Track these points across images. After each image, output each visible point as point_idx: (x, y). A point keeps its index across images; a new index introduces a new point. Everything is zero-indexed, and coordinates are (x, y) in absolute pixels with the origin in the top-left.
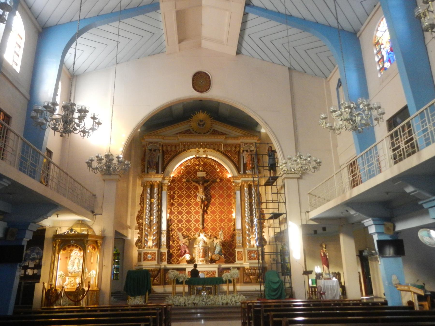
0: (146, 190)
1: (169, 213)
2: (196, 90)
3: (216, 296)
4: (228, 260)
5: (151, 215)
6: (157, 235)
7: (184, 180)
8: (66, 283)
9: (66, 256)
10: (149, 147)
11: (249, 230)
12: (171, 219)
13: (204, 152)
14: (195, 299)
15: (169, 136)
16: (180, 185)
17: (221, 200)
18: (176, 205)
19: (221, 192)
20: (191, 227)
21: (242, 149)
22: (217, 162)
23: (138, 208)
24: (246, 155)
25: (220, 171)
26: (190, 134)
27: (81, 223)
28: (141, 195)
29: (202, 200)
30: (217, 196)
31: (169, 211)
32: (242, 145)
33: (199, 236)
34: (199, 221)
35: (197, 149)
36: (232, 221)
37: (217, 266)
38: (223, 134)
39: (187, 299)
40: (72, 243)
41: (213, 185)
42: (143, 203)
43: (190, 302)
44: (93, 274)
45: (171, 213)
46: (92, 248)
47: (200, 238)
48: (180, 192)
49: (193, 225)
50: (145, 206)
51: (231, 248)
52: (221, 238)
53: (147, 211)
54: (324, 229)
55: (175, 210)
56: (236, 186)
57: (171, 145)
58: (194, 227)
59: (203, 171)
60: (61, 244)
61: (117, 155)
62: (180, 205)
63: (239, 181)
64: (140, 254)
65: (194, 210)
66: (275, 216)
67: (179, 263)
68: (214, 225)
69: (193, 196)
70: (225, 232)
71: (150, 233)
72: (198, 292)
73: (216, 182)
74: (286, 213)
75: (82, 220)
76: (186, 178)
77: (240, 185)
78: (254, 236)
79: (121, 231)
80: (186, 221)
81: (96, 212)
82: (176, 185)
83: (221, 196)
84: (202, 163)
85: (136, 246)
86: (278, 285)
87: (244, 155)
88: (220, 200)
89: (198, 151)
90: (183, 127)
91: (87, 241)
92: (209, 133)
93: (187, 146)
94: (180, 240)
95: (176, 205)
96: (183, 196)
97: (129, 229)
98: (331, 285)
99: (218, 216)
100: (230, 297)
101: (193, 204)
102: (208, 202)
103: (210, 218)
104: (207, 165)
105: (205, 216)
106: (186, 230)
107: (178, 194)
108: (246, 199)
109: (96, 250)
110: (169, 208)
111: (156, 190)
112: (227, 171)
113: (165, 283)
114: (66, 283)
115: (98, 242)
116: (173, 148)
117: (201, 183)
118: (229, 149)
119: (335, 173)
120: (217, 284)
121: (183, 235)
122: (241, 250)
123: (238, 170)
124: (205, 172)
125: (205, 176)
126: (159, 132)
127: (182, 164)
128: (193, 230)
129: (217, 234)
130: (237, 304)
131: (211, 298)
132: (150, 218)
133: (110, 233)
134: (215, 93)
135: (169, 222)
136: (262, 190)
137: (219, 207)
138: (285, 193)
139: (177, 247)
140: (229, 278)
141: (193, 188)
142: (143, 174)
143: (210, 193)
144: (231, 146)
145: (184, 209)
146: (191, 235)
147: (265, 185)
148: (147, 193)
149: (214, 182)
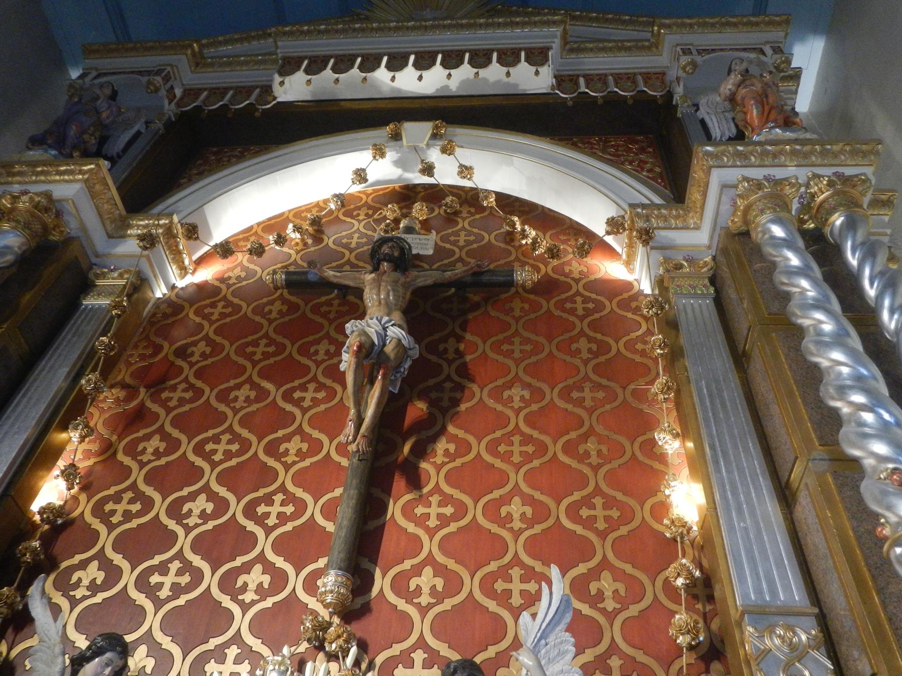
68: (471, 585)
87: (702, 113)
99: (516, 508)
102: (432, 403)
105: (395, 510)
137: (527, 440)
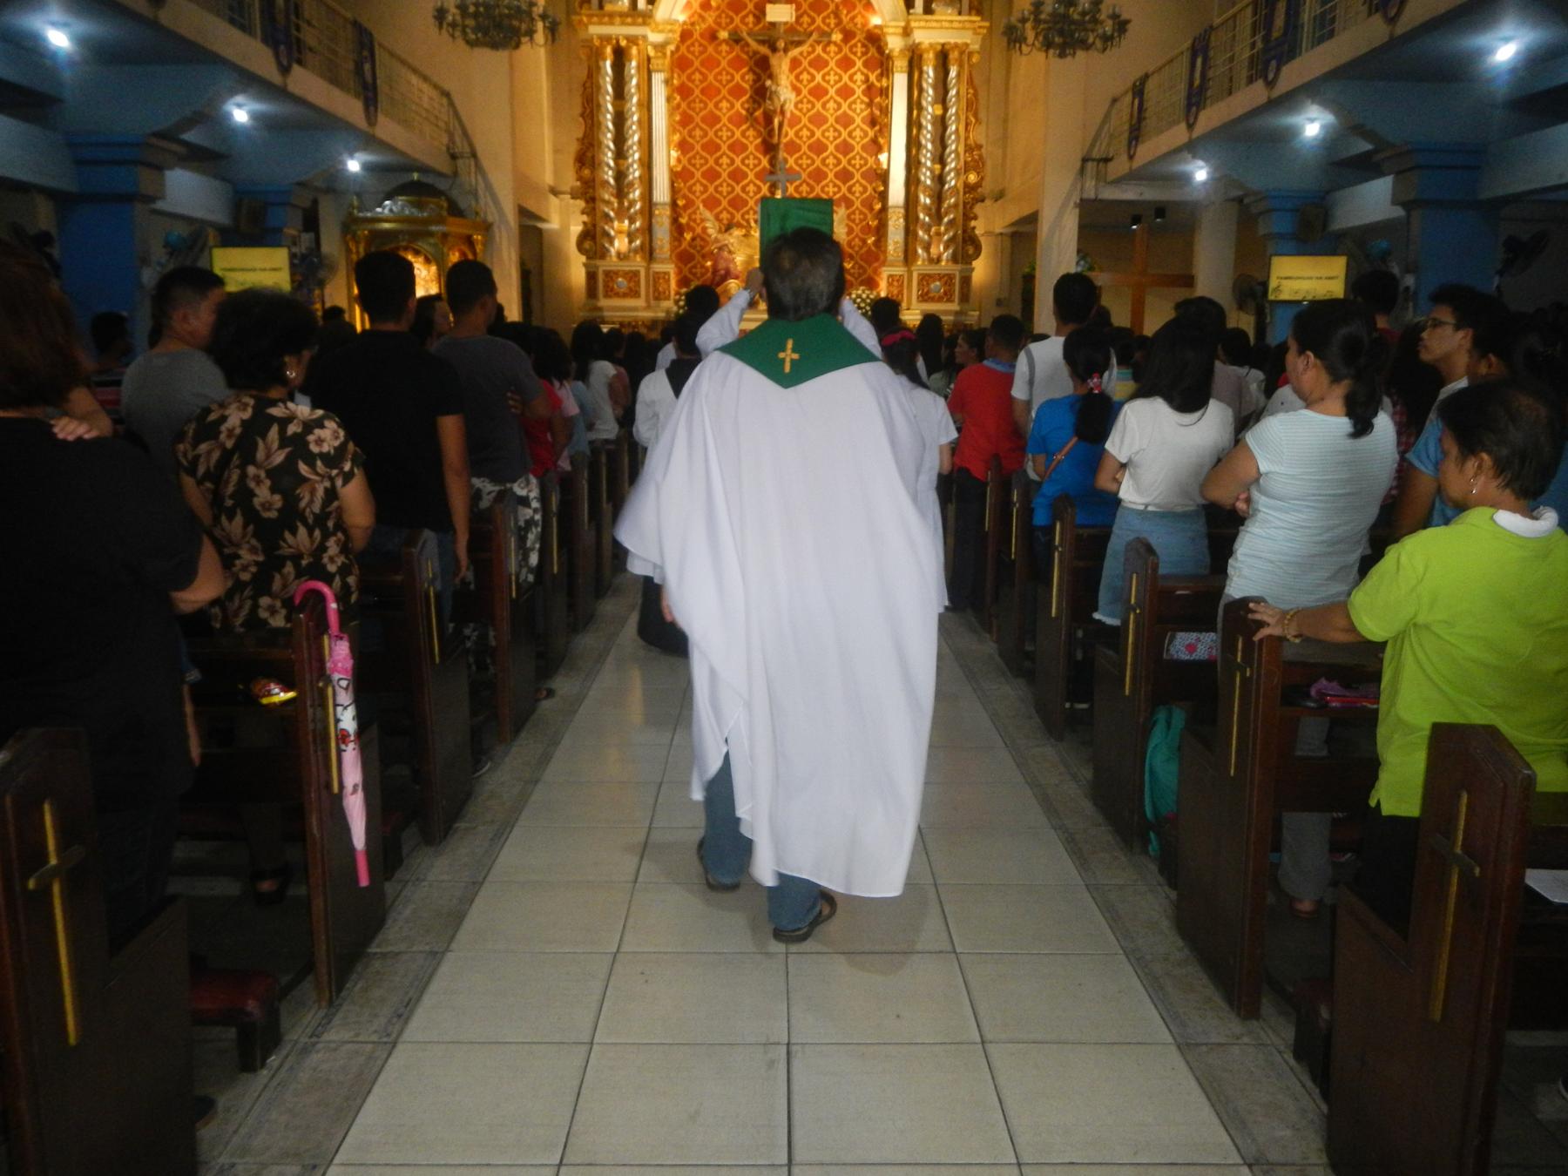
7: (724, 35)
17: (845, 107)
45: (683, 146)
49: (751, 188)
64: (591, 276)
79: (531, 206)
88: (839, 106)
96: (719, 92)
99: (831, 161)
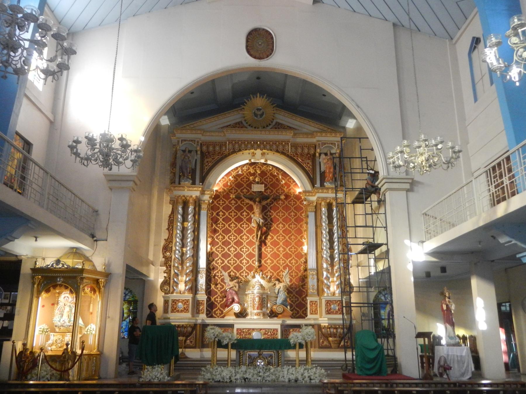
0: (177, 208)
1: (210, 244)
2: (251, 55)
3: (279, 368)
4: (296, 314)
5: (183, 246)
6: (191, 274)
7: (232, 196)
8: (50, 342)
9: (52, 302)
10: (182, 146)
11: (327, 270)
12: (213, 252)
13: (263, 154)
14: (246, 372)
15: (211, 130)
16: (227, 202)
17: (287, 226)
18: (220, 231)
19: (287, 214)
20: (242, 264)
21: (318, 150)
22: (282, 170)
23: (165, 235)
24: (324, 159)
25: (286, 184)
26: (242, 127)
27: (75, 252)
28: (170, 217)
29: (259, 225)
30: (281, 220)
31: (210, 240)
32: (319, 145)
33: (254, 277)
34: (254, 256)
35: (252, 151)
36: (302, 256)
37: (281, 322)
38: (290, 128)
39: (233, 372)
40: (60, 281)
41: (275, 203)
42: (173, 227)
43: (238, 376)
44: (91, 329)
45: (213, 244)
46: (91, 291)
47: (255, 280)
48: (227, 214)
49: (244, 261)
50: (175, 233)
51: (300, 295)
52: (287, 280)
53: (178, 240)
54: (443, 269)
55: (218, 239)
56: (309, 205)
57: (214, 144)
58: (246, 264)
59: (262, 183)
60: (43, 282)
61: (120, 136)
62: (226, 231)
63: (314, 199)
64: (166, 302)
65: (247, 239)
66: (370, 248)
67: (223, 317)
68: (275, 262)
69: (245, 220)
70: (292, 272)
71: (181, 273)
72: (252, 362)
73: (280, 199)
74: (387, 244)
75: (77, 248)
76: (235, 193)
77: (315, 204)
78: (335, 279)
79: (139, 269)
80: (235, 256)
81: (98, 235)
82: (221, 202)
83: (286, 220)
84: (259, 172)
85: (161, 290)
86: (376, 352)
87: (321, 160)
88: (284, 226)
89: (253, 153)
90: (232, 117)
91: (82, 279)
92: (271, 127)
93: (237, 146)
94: (225, 283)
95: (220, 231)
96: (231, 220)
97: (151, 265)
98: (459, 354)
99: (281, 249)
100: (301, 369)
101: (245, 232)
102: (267, 228)
103: (271, 251)
104: (266, 174)
105: (263, 249)
106: (235, 268)
107: (223, 216)
108: (324, 224)
109: (97, 293)
110: (211, 237)
111: (191, 209)
112: (296, 184)
113: (203, 345)
114: (50, 342)
115: (100, 282)
116: (217, 148)
117: (257, 199)
118: (300, 150)
119: (465, 182)
120: (280, 348)
121: (230, 276)
122: (316, 299)
123: (313, 182)
124: (263, 185)
125: (263, 190)
126: (196, 125)
127: (229, 172)
128: (244, 268)
129: (279, 276)
130: (312, 381)
131: (272, 371)
132: (182, 250)
133: (119, 270)
134: (281, 61)
135: (210, 256)
136: (349, 210)
137: (283, 236)
138: (385, 214)
139: (221, 293)
140: (300, 341)
141: (245, 208)
142: (173, 185)
143: (271, 216)
144: (303, 146)
145: (232, 238)
146: (242, 276)
147: (354, 202)
148: (179, 213)
149: (276, 199)
